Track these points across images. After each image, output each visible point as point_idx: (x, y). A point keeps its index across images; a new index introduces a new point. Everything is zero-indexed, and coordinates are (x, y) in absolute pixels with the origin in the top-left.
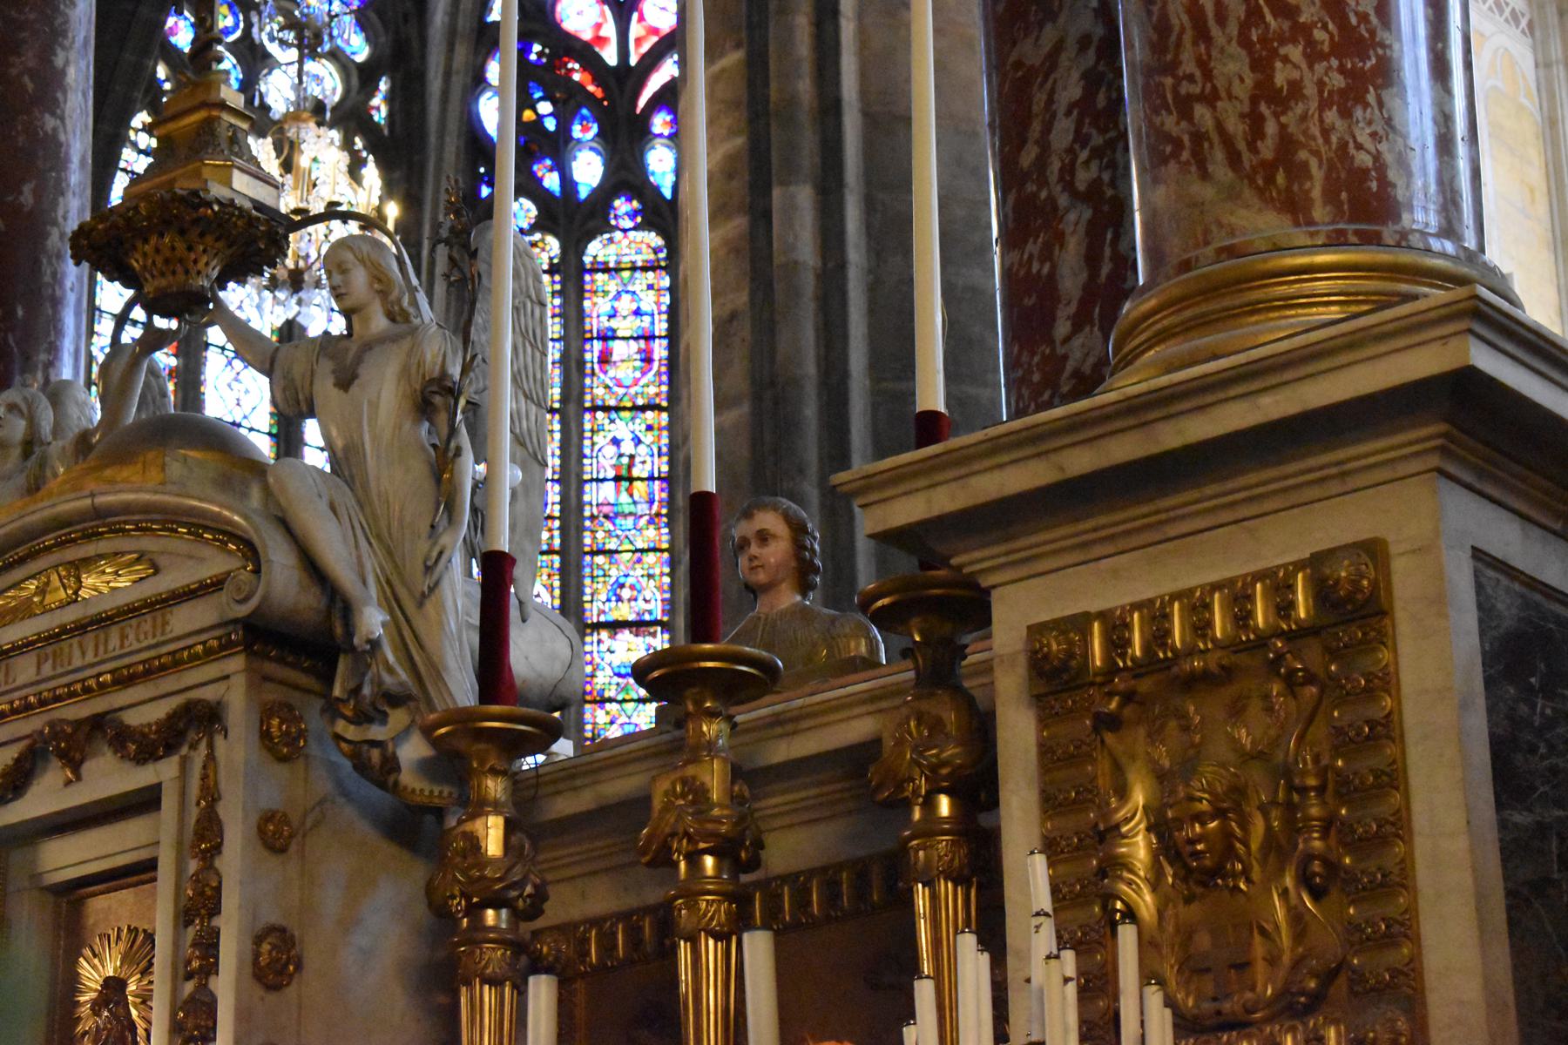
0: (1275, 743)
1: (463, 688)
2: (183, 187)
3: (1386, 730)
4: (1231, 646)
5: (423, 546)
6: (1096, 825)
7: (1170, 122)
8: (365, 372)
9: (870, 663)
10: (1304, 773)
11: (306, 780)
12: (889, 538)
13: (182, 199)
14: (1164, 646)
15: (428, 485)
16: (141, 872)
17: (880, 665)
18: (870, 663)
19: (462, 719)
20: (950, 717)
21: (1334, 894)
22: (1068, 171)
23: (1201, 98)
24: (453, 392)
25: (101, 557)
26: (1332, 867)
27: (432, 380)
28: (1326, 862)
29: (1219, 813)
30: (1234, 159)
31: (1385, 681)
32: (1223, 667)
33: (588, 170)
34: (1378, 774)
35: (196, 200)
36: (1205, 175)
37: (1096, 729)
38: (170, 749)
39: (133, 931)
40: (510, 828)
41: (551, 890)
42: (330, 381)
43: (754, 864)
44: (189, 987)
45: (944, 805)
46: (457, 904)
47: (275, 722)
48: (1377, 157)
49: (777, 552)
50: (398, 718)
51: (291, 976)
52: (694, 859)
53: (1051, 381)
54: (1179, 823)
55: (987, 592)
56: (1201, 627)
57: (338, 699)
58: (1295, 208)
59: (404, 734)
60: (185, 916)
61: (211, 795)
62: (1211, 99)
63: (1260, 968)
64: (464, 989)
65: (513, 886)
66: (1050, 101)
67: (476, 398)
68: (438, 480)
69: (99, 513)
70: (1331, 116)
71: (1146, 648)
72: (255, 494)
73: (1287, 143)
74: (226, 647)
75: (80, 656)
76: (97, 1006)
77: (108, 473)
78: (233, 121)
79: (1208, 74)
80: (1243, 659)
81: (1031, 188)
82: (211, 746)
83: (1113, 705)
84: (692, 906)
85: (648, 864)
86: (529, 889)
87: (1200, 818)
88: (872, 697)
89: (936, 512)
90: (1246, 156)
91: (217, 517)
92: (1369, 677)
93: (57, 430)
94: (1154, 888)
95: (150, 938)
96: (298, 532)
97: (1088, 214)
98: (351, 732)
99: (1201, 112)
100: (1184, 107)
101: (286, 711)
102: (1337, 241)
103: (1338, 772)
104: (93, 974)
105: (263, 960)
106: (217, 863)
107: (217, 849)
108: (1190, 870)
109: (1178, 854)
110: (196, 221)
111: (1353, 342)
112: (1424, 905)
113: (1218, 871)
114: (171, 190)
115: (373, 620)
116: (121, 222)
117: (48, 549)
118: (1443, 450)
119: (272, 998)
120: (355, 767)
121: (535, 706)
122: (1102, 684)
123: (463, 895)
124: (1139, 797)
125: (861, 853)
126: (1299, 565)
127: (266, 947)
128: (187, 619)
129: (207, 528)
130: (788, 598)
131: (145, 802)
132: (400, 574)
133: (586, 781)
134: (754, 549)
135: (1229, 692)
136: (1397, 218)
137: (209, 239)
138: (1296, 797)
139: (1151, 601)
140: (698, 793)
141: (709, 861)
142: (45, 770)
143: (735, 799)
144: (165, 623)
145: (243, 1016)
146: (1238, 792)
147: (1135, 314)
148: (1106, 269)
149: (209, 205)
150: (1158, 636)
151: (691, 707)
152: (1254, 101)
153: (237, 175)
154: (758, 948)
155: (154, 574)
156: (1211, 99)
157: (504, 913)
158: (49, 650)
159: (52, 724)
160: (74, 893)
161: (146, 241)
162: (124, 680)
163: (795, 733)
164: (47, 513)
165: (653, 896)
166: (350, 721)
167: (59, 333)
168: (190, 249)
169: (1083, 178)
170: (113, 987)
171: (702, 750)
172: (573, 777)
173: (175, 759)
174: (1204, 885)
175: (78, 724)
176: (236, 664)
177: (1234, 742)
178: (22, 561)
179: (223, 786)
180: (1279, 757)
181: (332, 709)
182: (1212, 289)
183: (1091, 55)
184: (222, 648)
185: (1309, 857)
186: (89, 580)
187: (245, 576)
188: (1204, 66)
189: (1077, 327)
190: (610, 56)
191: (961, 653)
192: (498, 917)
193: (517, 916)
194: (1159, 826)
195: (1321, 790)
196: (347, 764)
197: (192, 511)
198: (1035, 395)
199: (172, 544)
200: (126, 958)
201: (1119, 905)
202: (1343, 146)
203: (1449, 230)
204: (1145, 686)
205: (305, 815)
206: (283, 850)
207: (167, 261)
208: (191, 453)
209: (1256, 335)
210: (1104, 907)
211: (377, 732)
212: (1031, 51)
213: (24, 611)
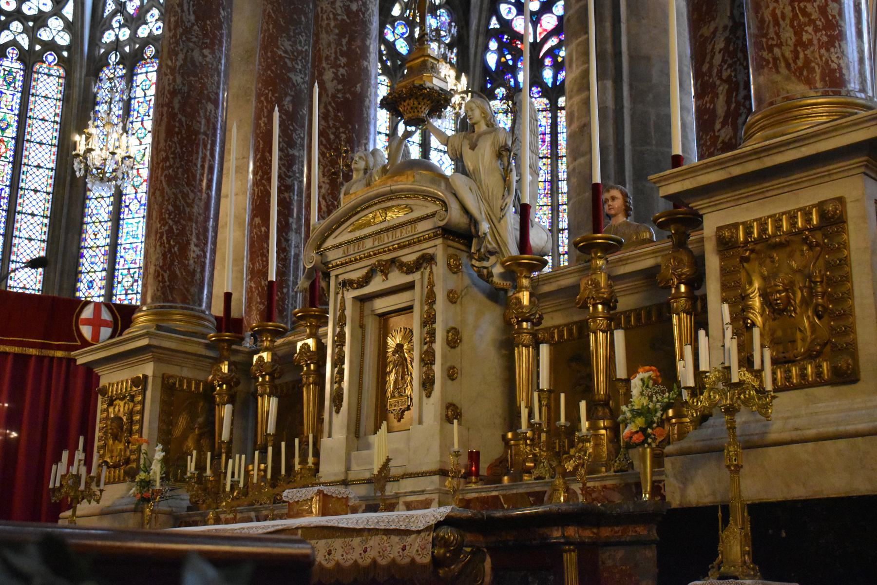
0: (805, 267)
1: (513, 250)
2: (417, 83)
3: (845, 262)
4: (789, 233)
5: (500, 202)
6: (741, 295)
7: (765, 54)
8: (481, 144)
9: (651, 241)
10: (816, 277)
11: (462, 279)
12: (668, 197)
13: (417, 87)
14: (765, 234)
15: (501, 182)
16: (409, 309)
17: (654, 241)
18: (651, 241)
19: (514, 259)
20: (685, 259)
21: (826, 318)
22: (720, 72)
23: (776, 45)
24: (509, 150)
25: (393, 206)
26: (825, 308)
27: (502, 147)
28: (823, 306)
29: (786, 290)
30: (788, 66)
31: (845, 245)
32: (786, 241)
34: (842, 277)
35: (422, 87)
36: (778, 72)
37: (741, 261)
38: (418, 269)
39: (405, 329)
40: (531, 295)
41: (544, 316)
42: (468, 147)
43: (615, 308)
44: (426, 347)
45: (683, 288)
46: (514, 320)
47: (452, 260)
48: (839, 65)
49: (618, 203)
50: (493, 259)
51: (458, 344)
52: (595, 306)
53: (714, 144)
54: (772, 294)
55: (701, 216)
56: (778, 227)
57: (473, 253)
58: (809, 82)
59: (495, 264)
60: (424, 324)
61: (431, 284)
62: (780, 45)
63: (799, 343)
64: (516, 349)
65: (532, 315)
66: (713, 48)
67: (516, 152)
68: (505, 180)
69: (392, 192)
70: (823, 51)
71: (759, 234)
72: (443, 185)
73: (807, 61)
74: (436, 236)
75: (387, 238)
76: (394, 353)
77: (395, 178)
78: (432, 61)
79: (779, 37)
80: (793, 238)
81: (706, 78)
82: (431, 268)
83: (747, 254)
84: (595, 322)
85: (580, 308)
86: (537, 316)
87: (779, 292)
88: (654, 252)
89: (685, 188)
90: (793, 65)
91: (434, 193)
92: (839, 244)
93: (374, 165)
94: (761, 316)
95: (411, 331)
96: (459, 197)
97: (727, 87)
98: (477, 264)
99: (776, 50)
100: (770, 49)
101: (456, 257)
102: (826, 94)
103: (827, 276)
104: (392, 343)
105: (450, 338)
106: (434, 307)
107: (434, 302)
108: (774, 309)
109: (771, 304)
110: (421, 95)
111: (835, 129)
112: (858, 322)
113: (785, 310)
114: (413, 84)
115: (485, 227)
116: (397, 95)
117: (376, 204)
118: (866, 166)
119: (453, 350)
120: (478, 275)
121: (536, 255)
122: (743, 247)
123: (516, 317)
124: (756, 285)
125: (648, 304)
126: (814, 206)
127: (450, 334)
128: (423, 226)
129: (429, 196)
130: (621, 219)
131: (410, 286)
132: (492, 212)
133: (554, 280)
134: (610, 203)
135: (788, 249)
136: (845, 86)
137: (425, 100)
138: (813, 285)
139: (761, 219)
140: (596, 285)
141: (600, 307)
142: (376, 276)
143: (610, 286)
144: (415, 228)
145: (444, 357)
146: (792, 283)
147: (753, 120)
148: (733, 105)
149: (426, 89)
150: (763, 230)
151: (593, 255)
152: (796, 45)
153: (434, 78)
154: (619, 336)
155: (412, 211)
156: (780, 45)
157: (529, 324)
158: (377, 237)
159: (378, 261)
160: (384, 317)
161: (405, 101)
162: (401, 247)
163: (626, 264)
164: (375, 192)
165: (576, 318)
166: (476, 260)
167: (369, 133)
168: (419, 104)
169: (725, 75)
170: (400, 347)
171: (595, 271)
172: (550, 279)
173: (419, 272)
174: (779, 314)
175: (386, 261)
176: (439, 241)
177: (791, 267)
178: (367, 208)
179: (435, 282)
180: (806, 271)
181: (471, 256)
182: (782, 111)
183: (727, 33)
184: (435, 236)
185: (817, 305)
186: (389, 214)
187: (443, 212)
188: (777, 34)
189: (723, 126)
191: (688, 236)
192: (527, 325)
193: (533, 324)
194: (764, 295)
195: (821, 282)
196: (475, 275)
197: (424, 191)
198: (708, 148)
200: (404, 338)
201: (749, 321)
202: (827, 61)
203: (863, 90)
204: (758, 247)
205: (462, 291)
206: (455, 303)
207: (412, 108)
208: (424, 172)
209: (799, 126)
210: (744, 322)
211: (485, 264)
212: (706, 31)
213: (368, 224)
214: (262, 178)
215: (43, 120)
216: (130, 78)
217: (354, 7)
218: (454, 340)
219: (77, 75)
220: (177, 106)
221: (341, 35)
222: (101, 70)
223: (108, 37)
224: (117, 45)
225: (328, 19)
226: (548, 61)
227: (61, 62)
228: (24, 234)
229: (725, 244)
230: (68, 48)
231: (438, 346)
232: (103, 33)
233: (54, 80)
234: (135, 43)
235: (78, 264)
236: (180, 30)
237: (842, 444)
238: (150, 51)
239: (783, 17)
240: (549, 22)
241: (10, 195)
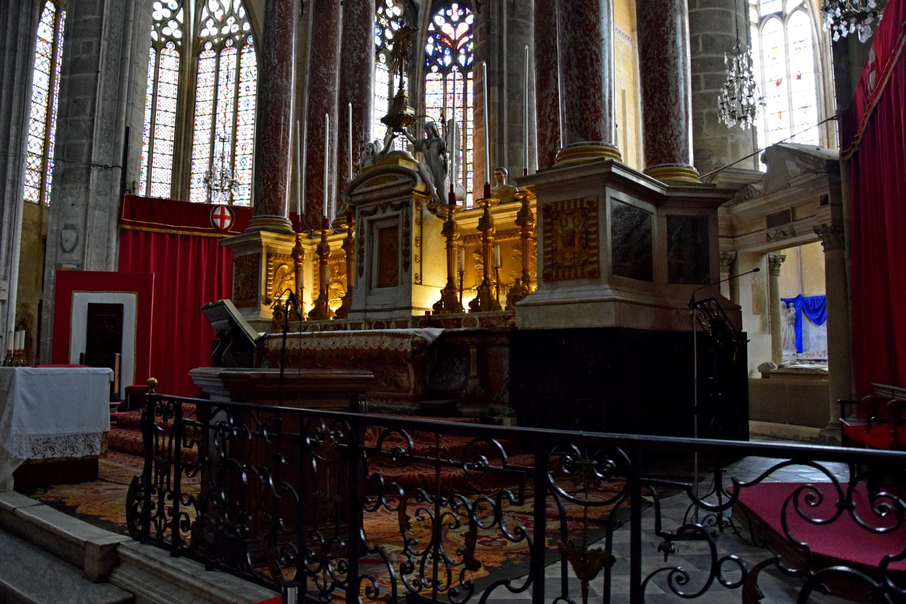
8: (432, 146)
22: (549, 116)
30: (577, 129)
36: (572, 131)
56: (569, 206)
70: (593, 123)
73: (586, 128)
156: (574, 119)
169: (552, 117)
199: (401, 175)
212: (544, 94)
214: (312, 144)
216: (218, 58)
217: (363, 56)
220: (269, 109)
221: (356, 72)
222: (200, 53)
223: (204, 34)
224: (209, 39)
225: (349, 62)
227: (177, 48)
228: (159, 151)
230: (181, 40)
232: (201, 30)
233: (173, 59)
234: (221, 37)
235: (191, 169)
236: (270, 68)
237: (589, 305)
238: (229, 43)
239: (576, 106)
241: (151, 129)
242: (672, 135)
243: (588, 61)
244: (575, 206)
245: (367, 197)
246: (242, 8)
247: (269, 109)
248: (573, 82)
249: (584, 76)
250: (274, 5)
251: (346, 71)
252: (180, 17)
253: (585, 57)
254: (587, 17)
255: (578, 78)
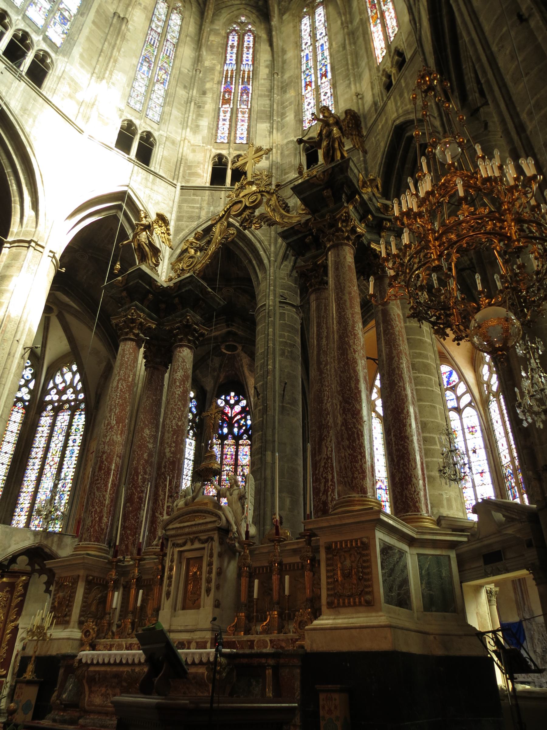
22: (322, 475)
30: (349, 485)
33: (225, 430)
35: (211, 468)
56: (346, 545)
61: (212, 549)
115: (235, 528)
145: (216, 580)
169: (324, 476)
176: (216, 532)
190: (230, 415)
215: (12, 432)
217: (180, 424)
218: (220, 573)
219: (31, 413)
221: (173, 435)
223: (48, 398)
224: (51, 402)
226: (236, 425)
227: (24, 407)
229: (329, 549)
230: (28, 401)
231: (213, 575)
236: (109, 427)
237: (369, 630)
240: (238, 409)
242: (415, 491)
243: (356, 436)
244: (352, 545)
245: (179, 532)
246: (80, 383)
247: (104, 458)
248: (345, 450)
249: (353, 446)
250: (118, 383)
251: (166, 434)
252: (32, 385)
253: (353, 433)
254: (354, 405)
255: (349, 448)
